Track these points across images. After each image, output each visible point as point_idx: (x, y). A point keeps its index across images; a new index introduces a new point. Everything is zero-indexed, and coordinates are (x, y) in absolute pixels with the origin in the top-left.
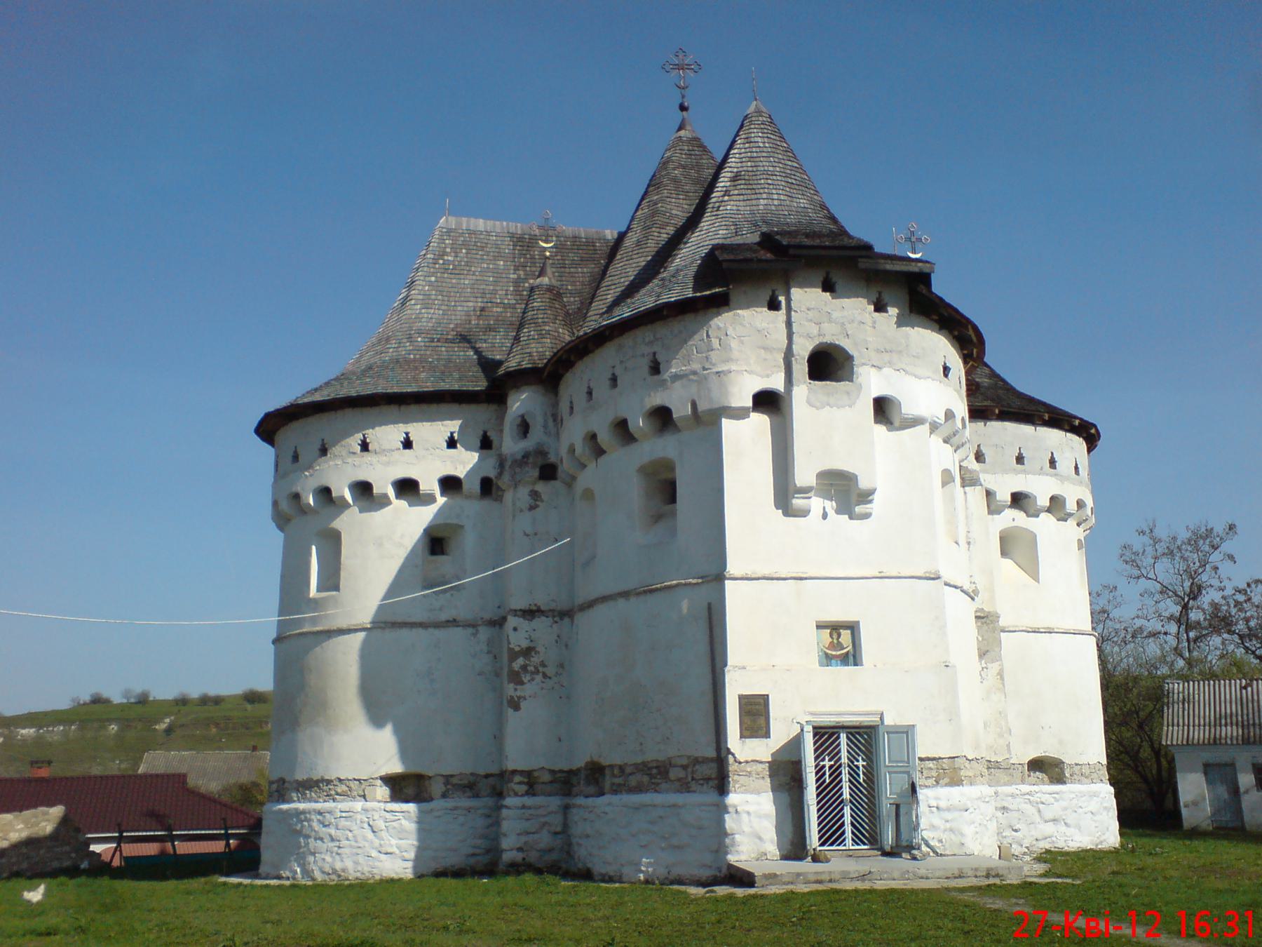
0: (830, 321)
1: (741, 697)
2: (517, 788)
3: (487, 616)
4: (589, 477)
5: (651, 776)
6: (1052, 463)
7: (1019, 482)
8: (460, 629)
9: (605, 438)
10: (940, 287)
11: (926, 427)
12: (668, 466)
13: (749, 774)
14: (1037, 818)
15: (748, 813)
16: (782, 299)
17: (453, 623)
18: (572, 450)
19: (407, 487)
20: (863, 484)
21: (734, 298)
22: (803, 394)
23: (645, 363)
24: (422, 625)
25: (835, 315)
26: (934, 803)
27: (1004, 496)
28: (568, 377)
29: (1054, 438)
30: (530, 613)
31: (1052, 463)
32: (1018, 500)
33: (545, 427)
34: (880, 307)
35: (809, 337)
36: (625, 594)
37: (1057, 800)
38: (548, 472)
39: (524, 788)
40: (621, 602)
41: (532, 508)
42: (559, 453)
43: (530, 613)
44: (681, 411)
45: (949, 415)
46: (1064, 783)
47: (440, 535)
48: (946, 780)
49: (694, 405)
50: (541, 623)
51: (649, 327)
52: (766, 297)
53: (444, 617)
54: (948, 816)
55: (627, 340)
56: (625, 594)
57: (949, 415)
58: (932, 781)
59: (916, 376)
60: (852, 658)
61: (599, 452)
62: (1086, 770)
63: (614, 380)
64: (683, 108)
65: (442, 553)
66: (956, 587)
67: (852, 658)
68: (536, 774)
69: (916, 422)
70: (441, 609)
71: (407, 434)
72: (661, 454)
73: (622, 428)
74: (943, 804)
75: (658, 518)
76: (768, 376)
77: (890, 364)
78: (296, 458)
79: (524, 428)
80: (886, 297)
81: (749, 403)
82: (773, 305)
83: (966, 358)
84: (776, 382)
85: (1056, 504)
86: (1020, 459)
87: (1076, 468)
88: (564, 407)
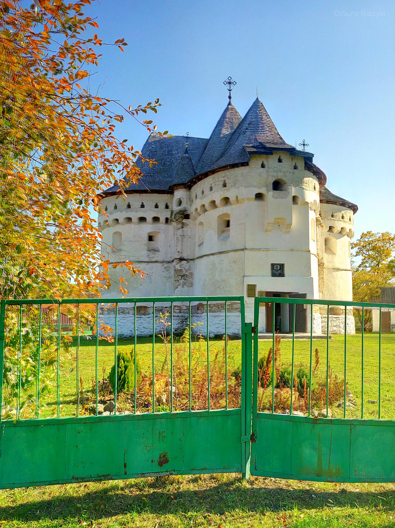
0: (281, 172)
2: (176, 311)
3: (167, 260)
4: (201, 218)
5: (219, 308)
8: (159, 264)
9: (207, 206)
10: (316, 162)
12: (227, 215)
16: (265, 163)
17: (156, 262)
18: (196, 210)
19: (142, 219)
21: (250, 163)
22: (270, 195)
23: (221, 183)
24: (148, 262)
28: (195, 187)
30: (181, 259)
33: (187, 202)
34: (295, 168)
36: (213, 254)
38: (187, 217)
39: (178, 311)
40: (211, 256)
41: (182, 227)
42: (191, 210)
43: (181, 259)
44: (232, 199)
45: (315, 201)
47: (151, 235)
49: (237, 197)
50: (184, 262)
51: (223, 172)
53: (154, 260)
55: (216, 175)
56: (213, 254)
57: (315, 201)
60: (282, 275)
61: (206, 211)
63: (211, 189)
64: (230, 97)
65: (152, 241)
68: (182, 307)
70: (153, 257)
71: (143, 203)
72: (225, 212)
73: (213, 203)
75: (223, 232)
78: (106, 209)
79: (180, 203)
81: (254, 197)
82: (263, 166)
83: (320, 184)
84: (262, 191)
88: (193, 196)
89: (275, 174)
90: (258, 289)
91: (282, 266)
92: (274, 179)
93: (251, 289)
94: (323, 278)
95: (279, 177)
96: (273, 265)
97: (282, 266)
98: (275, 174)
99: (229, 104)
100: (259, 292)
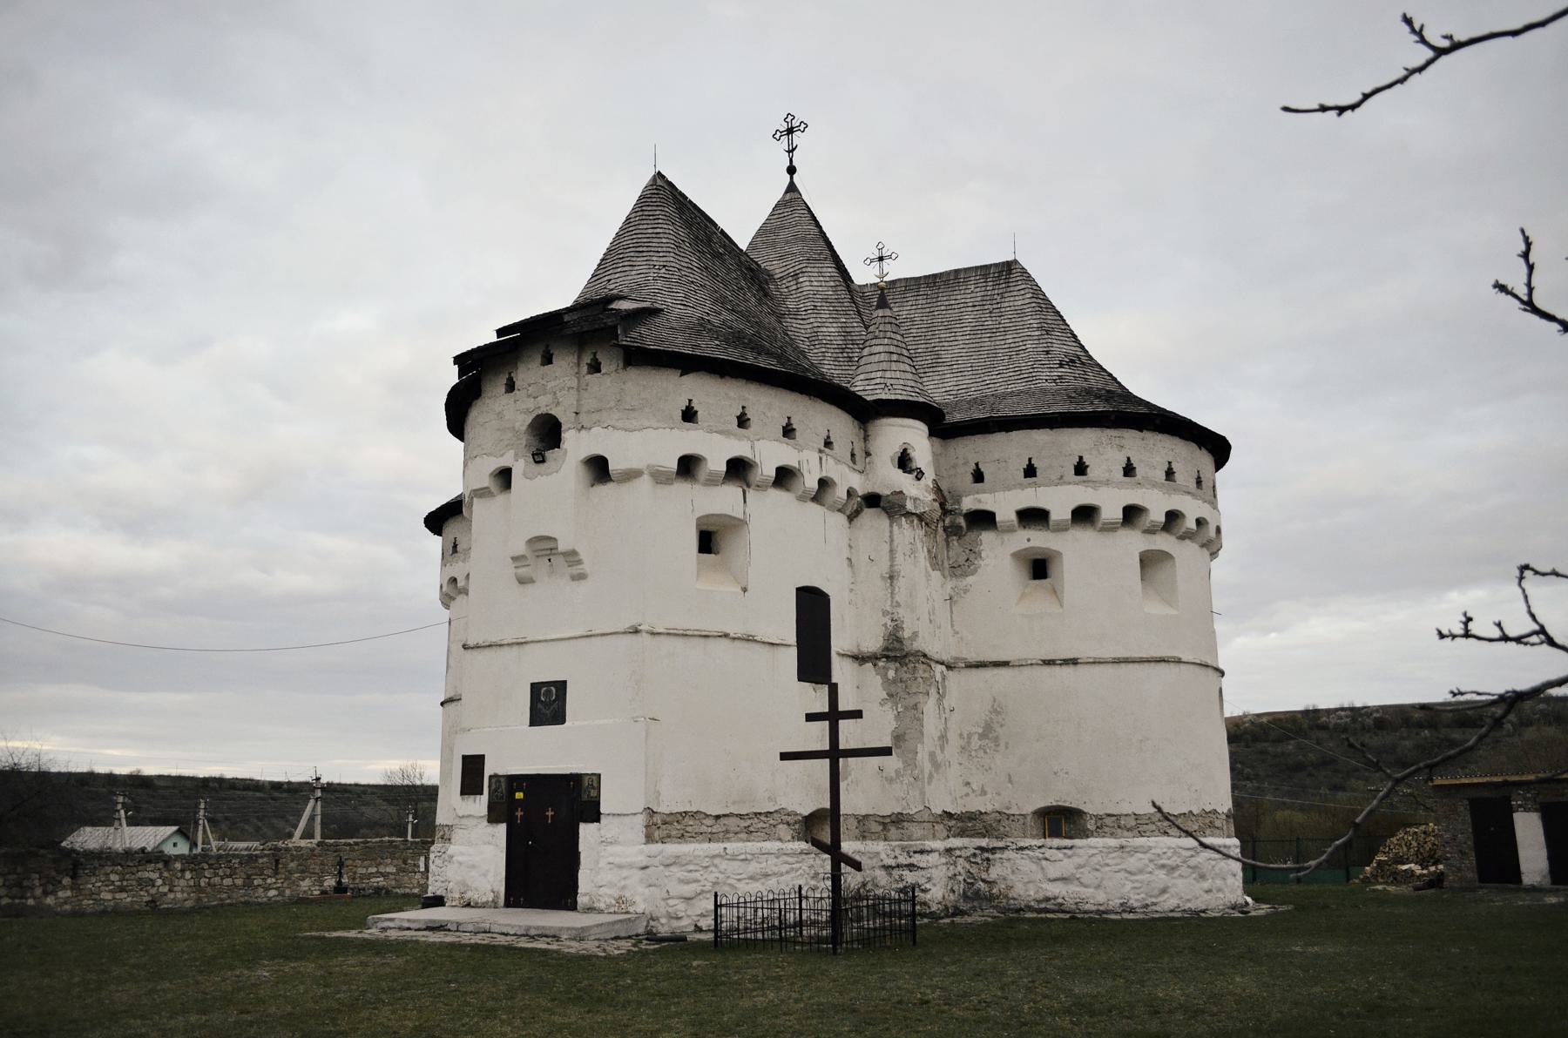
1: (464, 757)
6: (1081, 469)
11: (645, 482)
14: (1040, 876)
20: (562, 547)
22: (520, 467)
26: (611, 859)
29: (1081, 441)
31: (1081, 469)
32: (1033, 517)
34: (595, 368)
52: (503, 380)
54: (625, 873)
60: (558, 717)
64: (791, 170)
67: (558, 717)
69: (631, 475)
74: (617, 860)
77: (597, 423)
81: (485, 481)
85: (1085, 515)
86: (1030, 471)
87: (1129, 470)
89: (531, 404)
90: (489, 771)
91: (561, 686)
92: (529, 419)
93: (472, 768)
94: (915, 707)
95: (543, 410)
96: (536, 688)
97: (561, 686)
98: (531, 404)
99: (792, 188)
100: (491, 777)
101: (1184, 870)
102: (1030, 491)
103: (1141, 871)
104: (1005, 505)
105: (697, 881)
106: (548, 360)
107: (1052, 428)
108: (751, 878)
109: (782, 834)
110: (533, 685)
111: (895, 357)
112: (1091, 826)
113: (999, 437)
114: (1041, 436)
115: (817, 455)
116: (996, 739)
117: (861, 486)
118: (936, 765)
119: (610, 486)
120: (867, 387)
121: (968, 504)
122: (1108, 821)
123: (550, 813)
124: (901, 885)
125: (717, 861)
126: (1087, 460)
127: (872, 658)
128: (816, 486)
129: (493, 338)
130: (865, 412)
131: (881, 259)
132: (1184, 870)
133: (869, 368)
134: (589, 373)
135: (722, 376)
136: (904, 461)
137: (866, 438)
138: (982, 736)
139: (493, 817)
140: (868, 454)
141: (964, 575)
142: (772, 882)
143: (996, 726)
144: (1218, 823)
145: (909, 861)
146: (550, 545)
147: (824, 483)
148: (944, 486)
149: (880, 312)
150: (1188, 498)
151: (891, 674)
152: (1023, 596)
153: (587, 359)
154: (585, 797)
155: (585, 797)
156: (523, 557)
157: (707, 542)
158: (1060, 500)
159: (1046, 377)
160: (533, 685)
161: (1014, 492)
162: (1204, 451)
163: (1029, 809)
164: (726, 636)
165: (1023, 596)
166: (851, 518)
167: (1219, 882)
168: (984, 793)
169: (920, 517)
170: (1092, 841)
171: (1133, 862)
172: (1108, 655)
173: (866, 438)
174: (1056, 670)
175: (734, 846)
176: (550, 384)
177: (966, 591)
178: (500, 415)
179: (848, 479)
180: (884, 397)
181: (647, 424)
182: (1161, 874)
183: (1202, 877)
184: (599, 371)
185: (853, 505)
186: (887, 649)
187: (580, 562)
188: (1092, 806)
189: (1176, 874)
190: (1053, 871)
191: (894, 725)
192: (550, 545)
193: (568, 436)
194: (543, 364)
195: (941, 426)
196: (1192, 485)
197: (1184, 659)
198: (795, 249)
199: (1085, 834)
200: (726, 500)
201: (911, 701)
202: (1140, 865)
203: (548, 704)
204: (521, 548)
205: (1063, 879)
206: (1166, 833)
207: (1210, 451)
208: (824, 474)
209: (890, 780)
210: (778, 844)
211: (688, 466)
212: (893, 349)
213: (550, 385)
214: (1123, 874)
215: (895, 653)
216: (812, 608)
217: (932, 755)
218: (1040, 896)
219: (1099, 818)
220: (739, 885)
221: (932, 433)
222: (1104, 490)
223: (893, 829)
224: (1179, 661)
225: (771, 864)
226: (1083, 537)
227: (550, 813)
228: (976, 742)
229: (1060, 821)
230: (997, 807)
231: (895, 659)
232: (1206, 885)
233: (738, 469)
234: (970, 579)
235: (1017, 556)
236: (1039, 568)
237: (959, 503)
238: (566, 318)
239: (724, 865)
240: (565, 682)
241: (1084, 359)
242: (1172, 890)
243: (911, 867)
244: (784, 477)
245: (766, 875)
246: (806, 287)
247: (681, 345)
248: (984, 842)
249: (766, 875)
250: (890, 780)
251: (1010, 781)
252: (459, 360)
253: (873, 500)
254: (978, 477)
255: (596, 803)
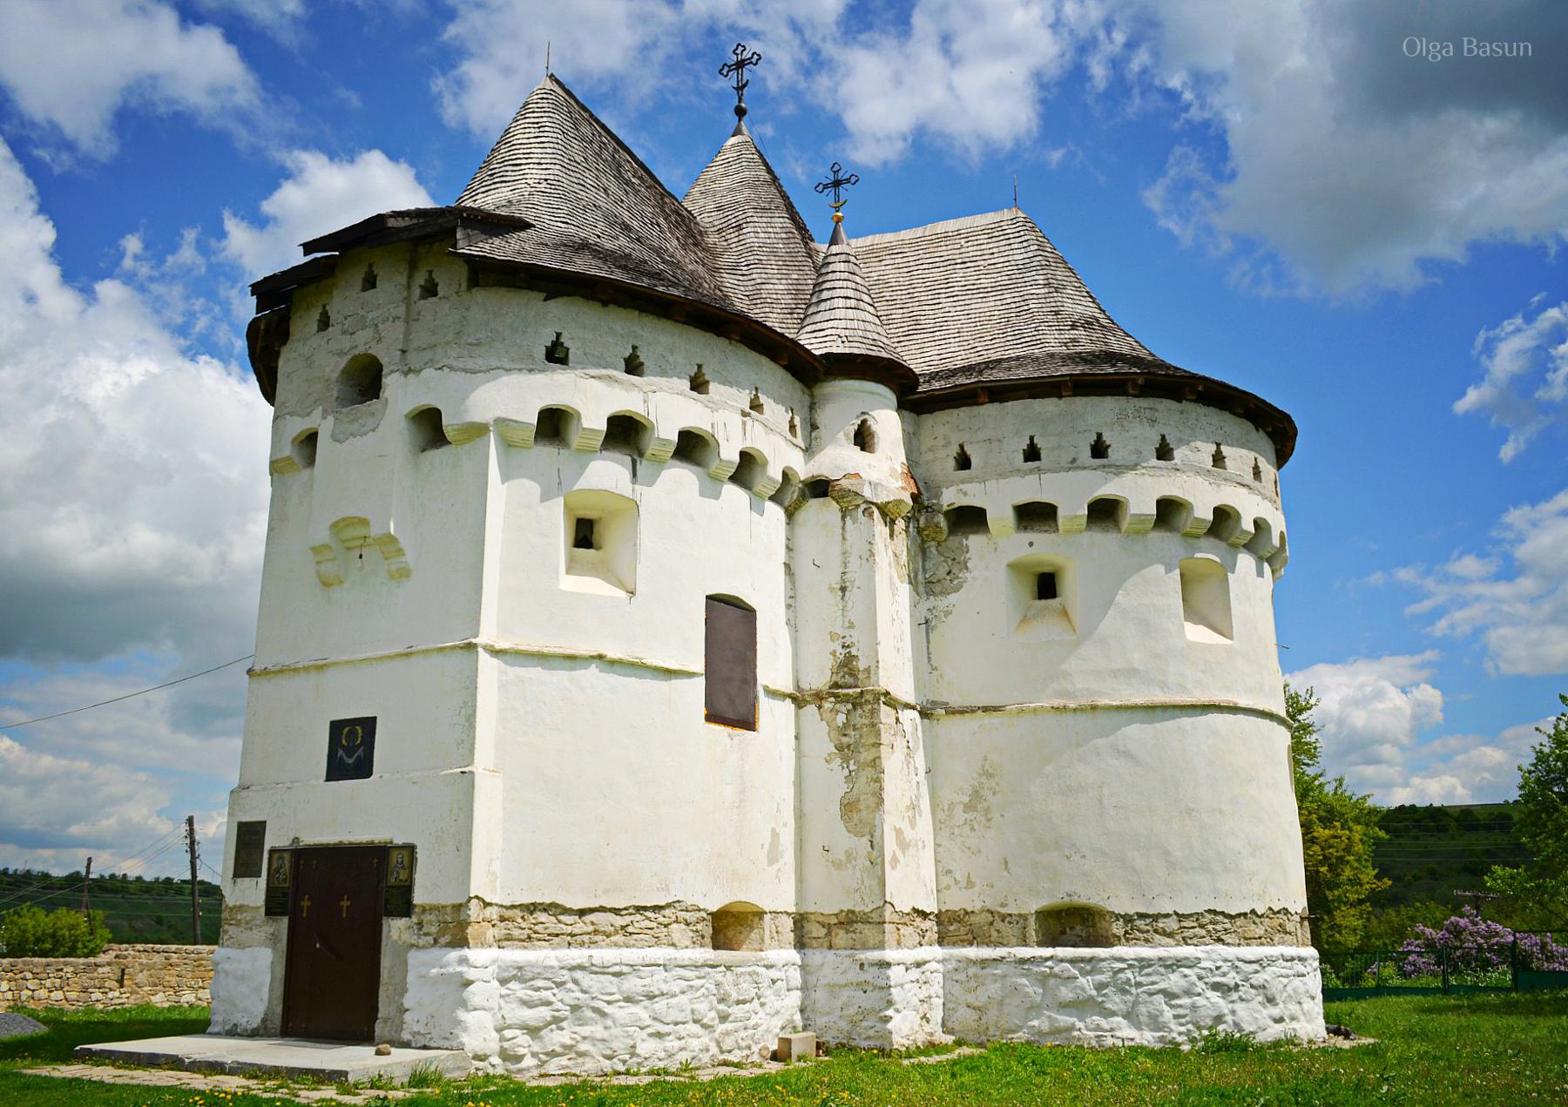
6: (1099, 450)
7: (1031, 489)
13: (238, 924)
15: (227, 973)
20: (375, 531)
25: (370, 316)
27: (1000, 516)
29: (1100, 413)
31: (1099, 450)
32: (1035, 515)
34: (430, 290)
35: (341, 353)
37: (1084, 973)
46: (1112, 945)
48: (447, 938)
52: (315, 315)
58: (430, 939)
59: (466, 371)
60: (363, 769)
62: (1172, 924)
66: (572, 658)
67: (363, 769)
76: (308, 414)
80: (437, 277)
86: (1032, 454)
89: (346, 343)
91: (369, 724)
92: (343, 362)
94: (875, 763)
95: (361, 350)
96: (336, 727)
97: (369, 724)
98: (346, 343)
100: (272, 851)
101: (1245, 990)
102: (1033, 478)
103: (1188, 993)
104: (998, 497)
105: (549, 1003)
106: (370, 283)
107: (1060, 397)
108: (628, 1000)
109: (676, 937)
110: (333, 724)
111: (853, 303)
112: (1118, 928)
113: (990, 410)
114: (1048, 406)
115: (739, 418)
116: (987, 810)
117: (804, 470)
118: (903, 845)
119: (445, 450)
120: (816, 345)
121: (951, 497)
122: (1140, 923)
123: (345, 903)
124: (852, 1011)
125: (578, 975)
126: (1107, 438)
127: (819, 697)
128: (737, 459)
129: (299, 258)
130: (810, 372)
131: (837, 184)
132: (1245, 990)
133: (818, 318)
134: (423, 297)
135: (605, 304)
136: (863, 438)
137: (812, 407)
138: (968, 808)
139: (273, 907)
140: (814, 427)
141: (945, 593)
142: (660, 1005)
143: (986, 793)
144: (1290, 927)
145: (863, 977)
146: (361, 531)
147: (747, 459)
148: (918, 472)
149: (835, 249)
150: (1244, 490)
151: (841, 719)
152: (1025, 620)
153: (420, 279)
154: (392, 881)
155: (392, 881)
156: (326, 546)
157: (585, 534)
158: (1071, 493)
159: (1053, 341)
160: (333, 724)
161: (1012, 480)
162: (1261, 433)
163: (1033, 906)
164: (601, 657)
165: (1025, 620)
166: (790, 514)
167: (1294, 1008)
168: (970, 884)
169: (883, 510)
170: (1118, 951)
171: (1174, 981)
172: (1139, 700)
173: (812, 407)
174: (1069, 719)
175: (604, 954)
176: (366, 316)
177: (947, 614)
178: (309, 362)
179: (783, 456)
180: (835, 350)
181: (495, 363)
182: (1214, 996)
183: (1271, 1000)
184: (435, 294)
185: (793, 494)
186: (836, 685)
187: (400, 552)
188: (1121, 903)
189: (1235, 996)
190: (1066, 993)
191: (844, 788)
192: (361, 531)
193: (392, 383)
194: (364, 289)
195: (915, 396)
196: (1248, 477)
197: (1242, 703)
198: (740, 198)
199: (1106, 942)
200: (607, 474)
201: (866, 756)
202: (1183, 982)
203: (351, 749)
204: (322, 535)
205: (1081, 1006)
206: (1219, 940)
207: (1269, 435)
208: (747, 444)
209: (838, 865)
210: (671, 952)
211: (553, 424)
212: (850, 293)
213: (370, 316)
214: (1160, 998)
215: (849, 695)
216: (729, 621)
217: (899, 832)
218: (1045, 1027)
219: (1128, 919)
220: (608, 1009)
221: (902, 406)
222: (1129, 476)
223: (842, 933)
224: (1234, 709)
225: (658, 980)
226: (1103, 540)
227: (345, 903)
228: (960, 816)
229: (1071, 924)
230: (989, 905)
231: (845, 699)
232: (1275, 1012)
233: (625, 433)
234: (953, 598)
235: (1016, 568)
236: (1047, 585)
237: (938, 496)
238: (392, 223)
239: (586, 979)
240: (374, 719)
241: (1104, 321)
242: (1229, 1018)
243: (863, 987)
244: (691, 446)
245: (651, 997)
246: (750, 239)
247: (548, 260)
248: (972, 952)
249: (651, 997)
250: (838, 865)
251: (1006, 868)
252: (257, 289)
253: (819, 488)
254: (964, 462)
255: (408, 889)
